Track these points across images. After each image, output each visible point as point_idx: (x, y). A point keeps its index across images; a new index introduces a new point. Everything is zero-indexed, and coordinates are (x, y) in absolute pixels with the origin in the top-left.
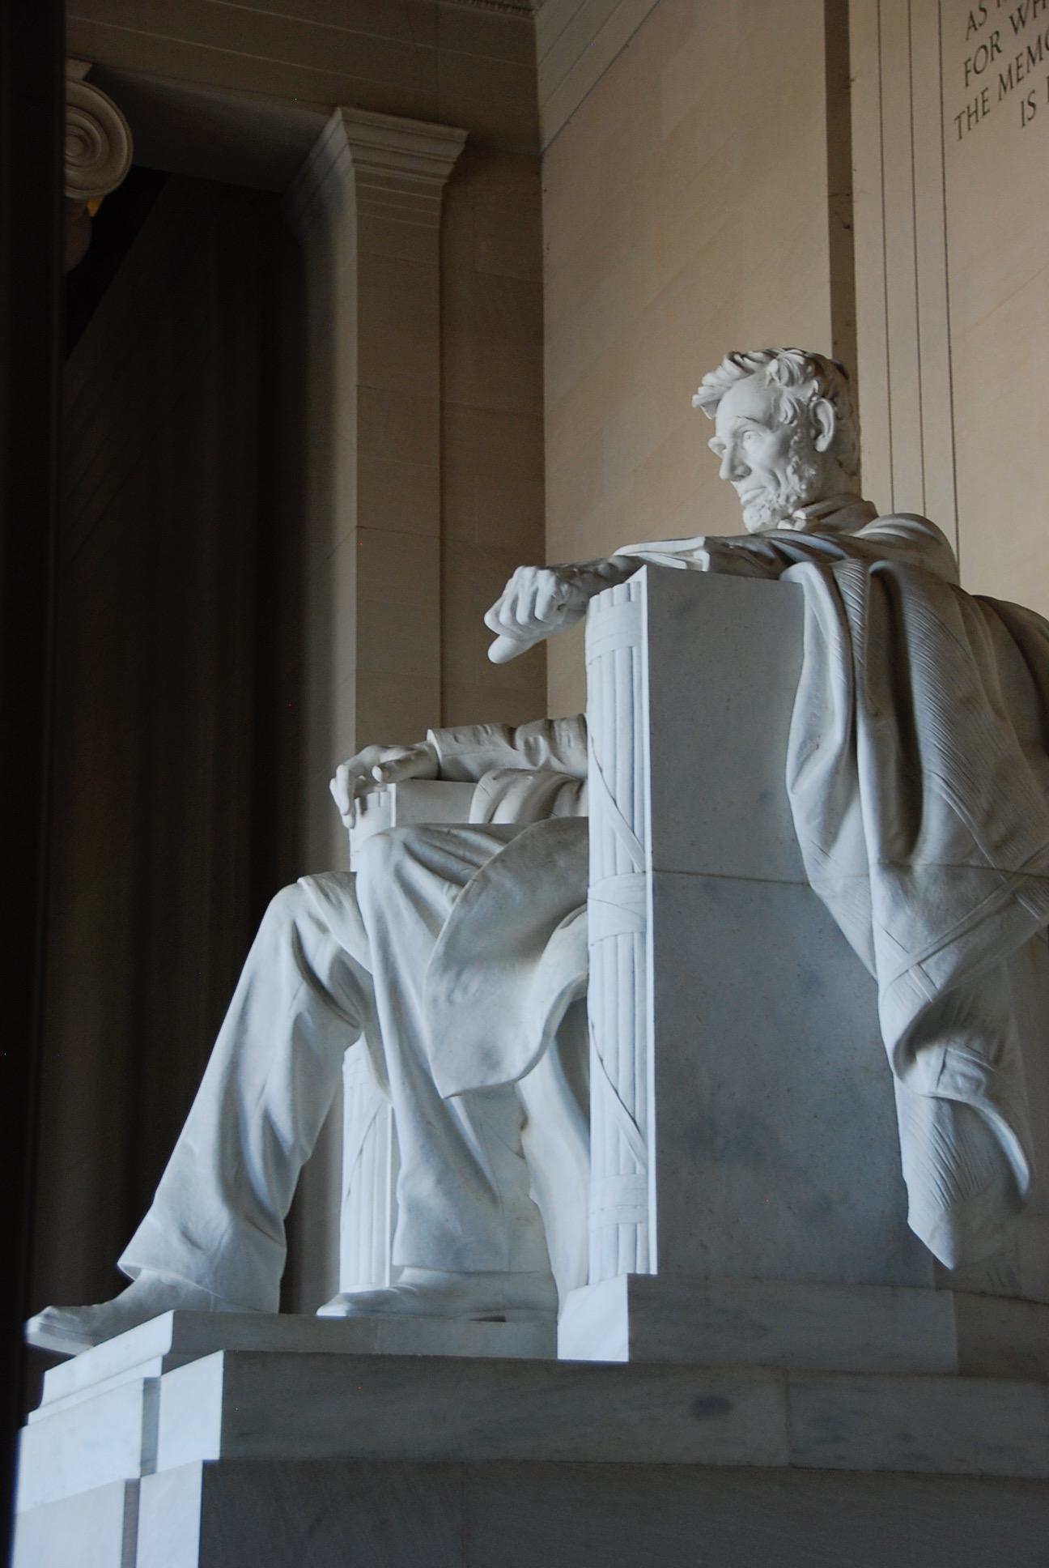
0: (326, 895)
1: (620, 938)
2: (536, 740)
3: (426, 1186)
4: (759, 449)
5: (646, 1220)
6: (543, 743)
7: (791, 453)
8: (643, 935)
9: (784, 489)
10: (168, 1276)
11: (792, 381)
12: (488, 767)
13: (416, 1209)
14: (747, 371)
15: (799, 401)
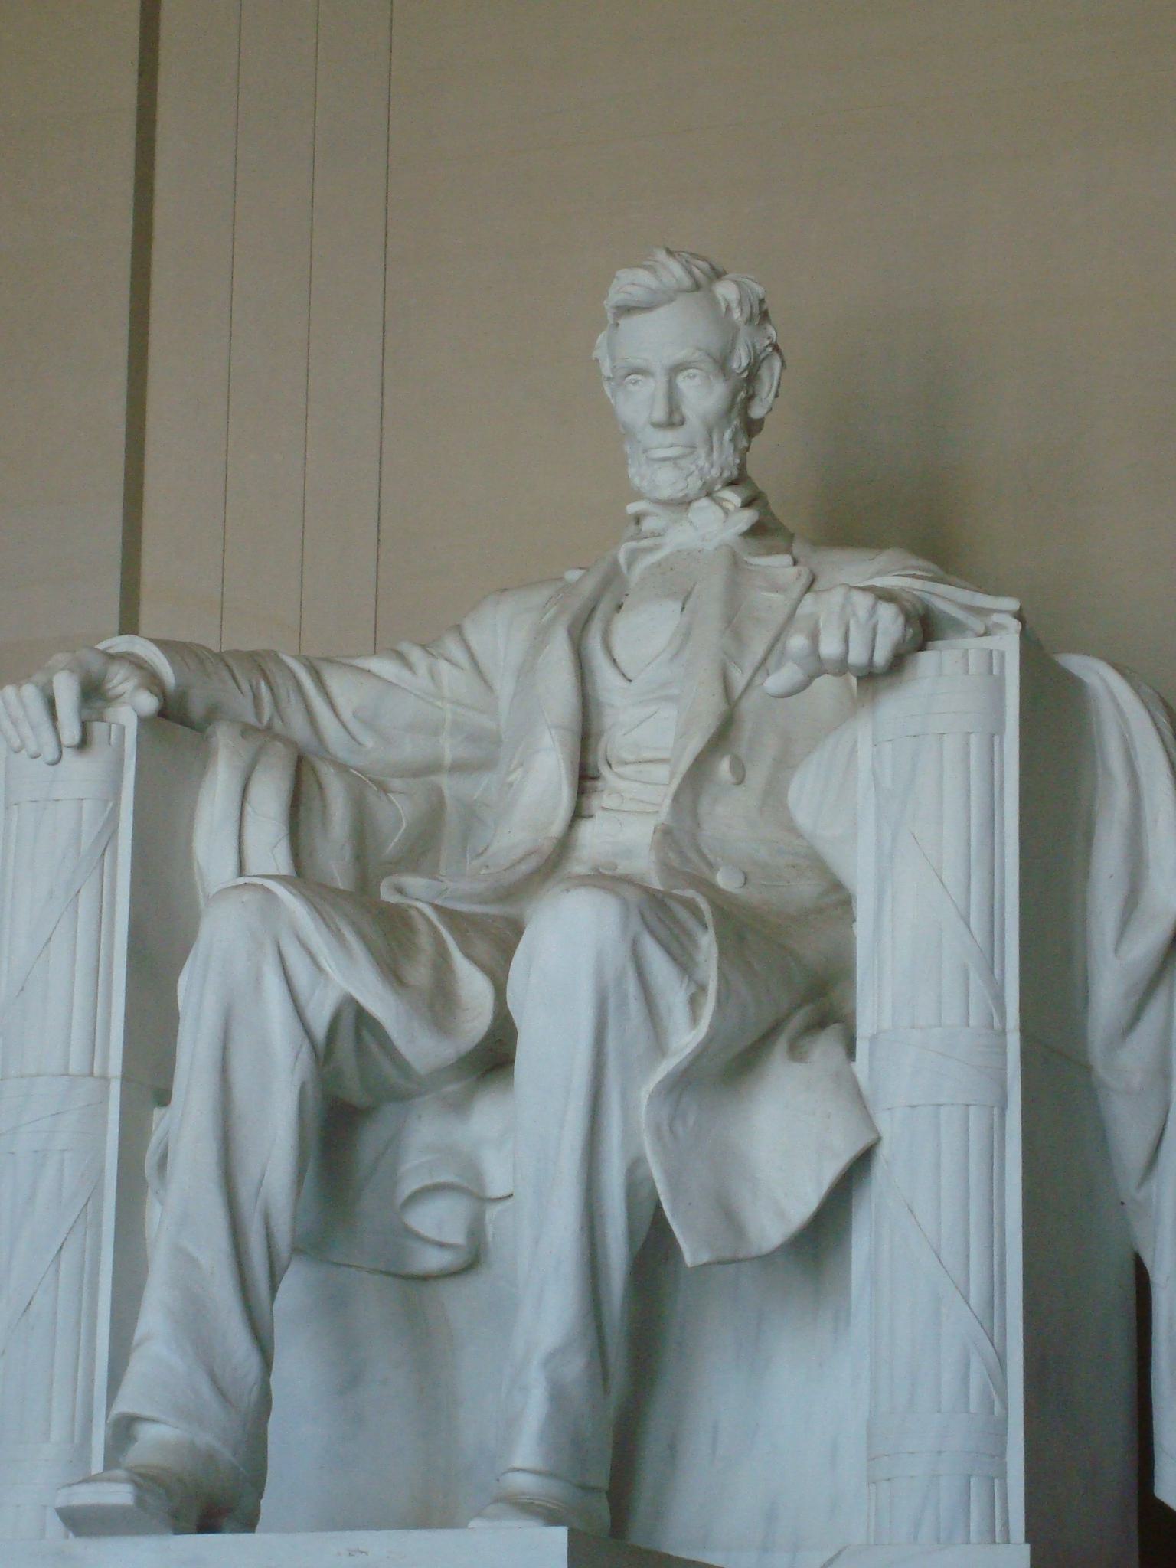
0: (321, 915)
1: (972, 1109)
2: (258, 684)
3: (575, 1367)
4: (702, 397)
5: (1003, 1476)
6: (263, 686)
7: (735, 411)
8: (1003, 1109)
9: (715, 455)
10: (206, 1439)
11: (750, 320)
12: (213, 714)
13: (557, 1396)
14: (697, 286)
15: (754, 347)
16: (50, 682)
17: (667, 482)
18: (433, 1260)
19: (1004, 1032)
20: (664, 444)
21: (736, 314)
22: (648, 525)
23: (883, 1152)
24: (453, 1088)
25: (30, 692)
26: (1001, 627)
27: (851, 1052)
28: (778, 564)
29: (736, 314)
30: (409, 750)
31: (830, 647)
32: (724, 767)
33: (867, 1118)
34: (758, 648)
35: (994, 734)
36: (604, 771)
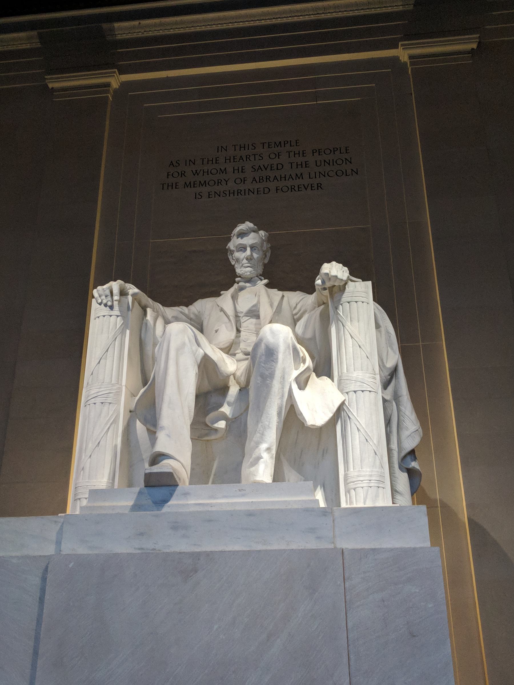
27: (333, 381)
28: (275, 291)
29: (264, 238)
34: (276, 304)
36: (241, 329)
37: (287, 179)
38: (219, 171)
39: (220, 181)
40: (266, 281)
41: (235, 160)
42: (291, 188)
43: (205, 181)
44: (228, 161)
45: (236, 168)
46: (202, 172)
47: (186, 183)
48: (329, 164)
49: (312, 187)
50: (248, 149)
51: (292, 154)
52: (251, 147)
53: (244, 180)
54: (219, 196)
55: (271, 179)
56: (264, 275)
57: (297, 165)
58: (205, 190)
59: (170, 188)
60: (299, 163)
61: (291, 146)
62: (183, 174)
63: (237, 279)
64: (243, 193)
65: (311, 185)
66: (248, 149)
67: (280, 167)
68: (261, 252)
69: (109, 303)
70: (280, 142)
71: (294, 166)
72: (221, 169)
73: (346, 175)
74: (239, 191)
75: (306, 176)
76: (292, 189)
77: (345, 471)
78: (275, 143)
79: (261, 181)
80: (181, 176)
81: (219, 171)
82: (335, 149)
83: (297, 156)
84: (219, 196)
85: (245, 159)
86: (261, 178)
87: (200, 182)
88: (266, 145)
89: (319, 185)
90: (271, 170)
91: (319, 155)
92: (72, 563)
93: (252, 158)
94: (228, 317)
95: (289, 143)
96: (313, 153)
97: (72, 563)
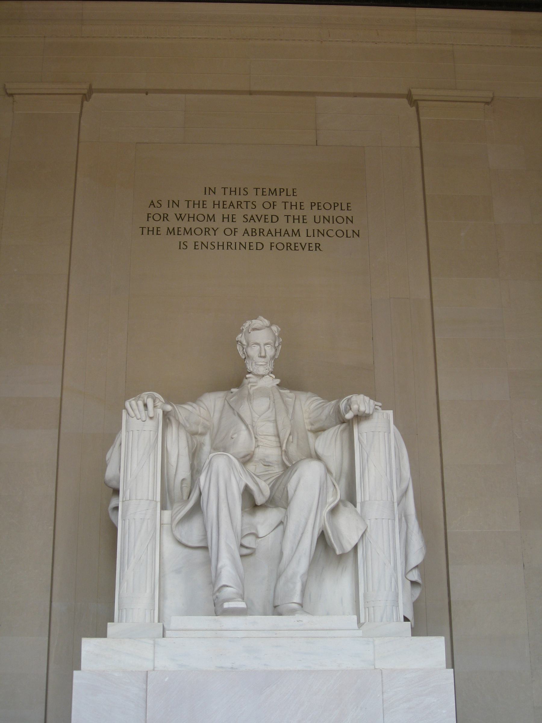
4: (270, 351)
5: (398, 606)
16: (144, 401)
17: (261, 370)
18: (245, 551)
19: (393, 503)
20: (261, 361)
21: (276, 334)
22: (251, 380)
23: (368, 529)
24: (247, 510)
25: (140, 403)
26: (376, 409)
29: (276, 334)
30: (194, 428)
31: (362, 409)
32: (291, 437)
33: (364, 521)
34: (291, 411)
35: (390, 433)
36: (257, 437)
37: (282, 234)
38: (206, 218)
39: (207, 230)
40: (278, 381)
41: (225, 206)
42: (287, 246)
43: (191, 229)
44: (216, 206)
45: (226, 216)
46: (187, 216)
47: (168, 229)
48: (329, 221)
49: (309, 247)
50: (240, 194)
51: (288, 205)
52: (242, 192)
53: (235, 232)
54: (207, 248)
55: (265, 233)
56: (276, 372)
57: (294, 219)
58: (190, 239)
59: (151, 233)
60: (296, 217)
61: (287, 195)
62: (165, 217)
63: (248, 376)
64: (233, 246)
65: (309, 244)
66: (240, 194)
67: (275, 219)
68: (274, 350)
69: (144, 420)
70: (275, 190)
71: (291, 219)
72: (208, 215)
73: (347, 237)
74: (229, 244)
75: (303, 233)
76: (288, 246)
77: (365, 591)
78: (270, 190)
79: (254, 234)
80: (164, 220)
81: (206, 218)
82: (336, 205)
83: (294, 207)
84: (207, 248)
85: (236, 207)
86: (254, 230)
87: (185, 229)
88: (260, 192)
89: (318, 245)
90: (265, 222)
91: (318, 209)
92: (167, 678)
93: (244, 205)
94: (247, 426)
95: (285, 190)
96: (312, 206)
97: (167, 678)
